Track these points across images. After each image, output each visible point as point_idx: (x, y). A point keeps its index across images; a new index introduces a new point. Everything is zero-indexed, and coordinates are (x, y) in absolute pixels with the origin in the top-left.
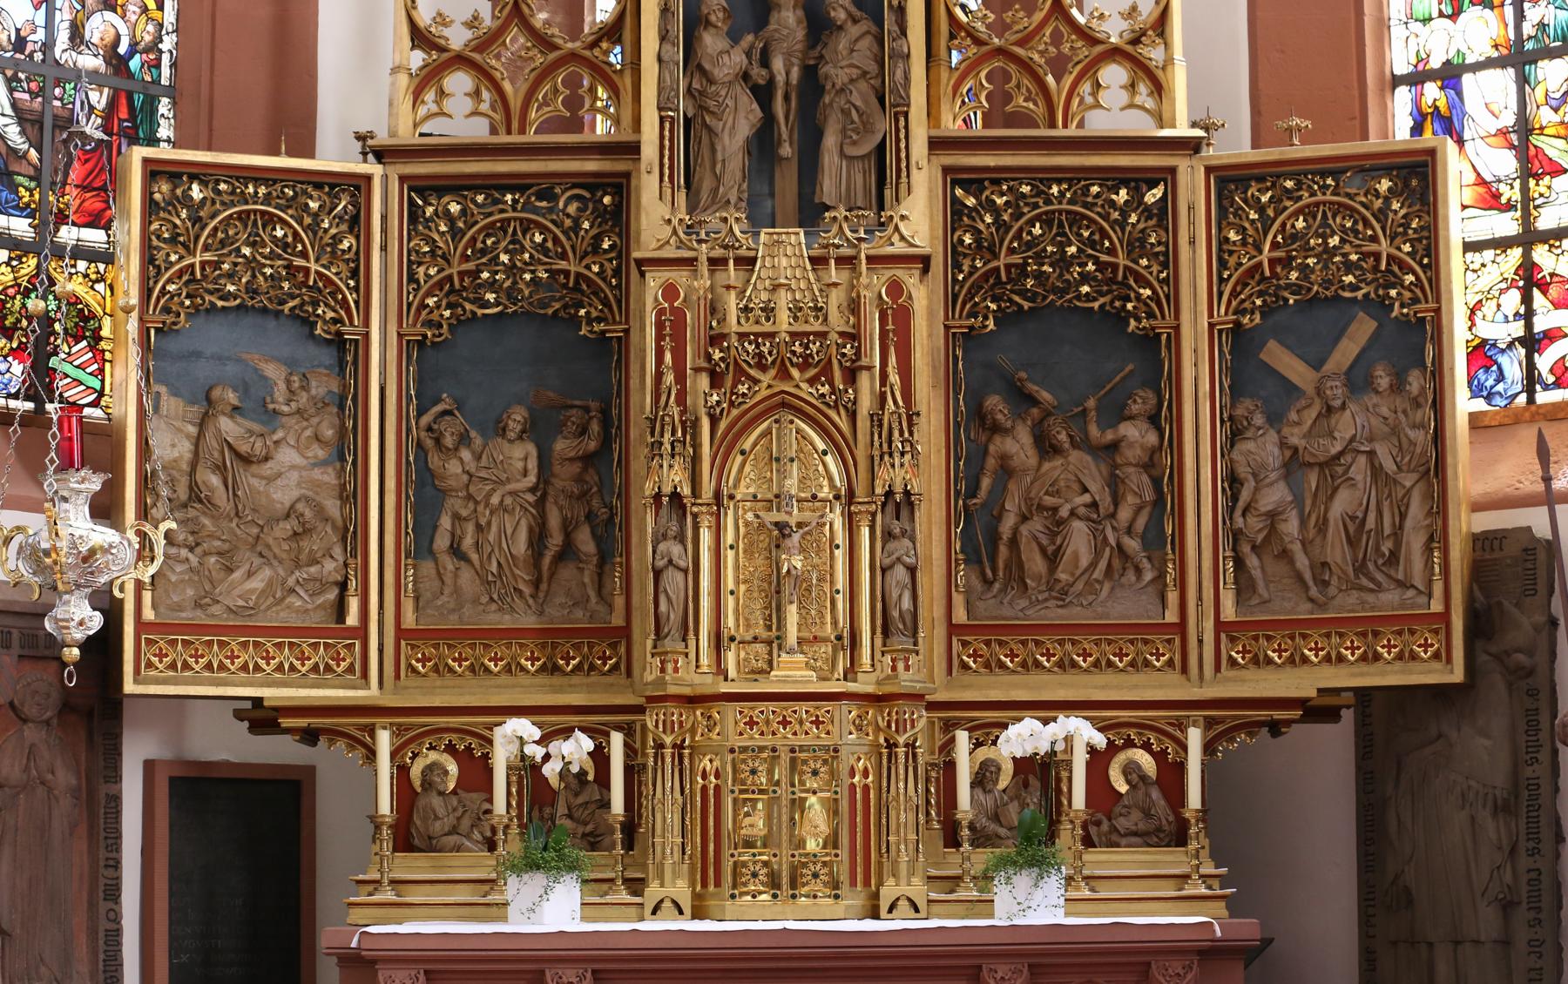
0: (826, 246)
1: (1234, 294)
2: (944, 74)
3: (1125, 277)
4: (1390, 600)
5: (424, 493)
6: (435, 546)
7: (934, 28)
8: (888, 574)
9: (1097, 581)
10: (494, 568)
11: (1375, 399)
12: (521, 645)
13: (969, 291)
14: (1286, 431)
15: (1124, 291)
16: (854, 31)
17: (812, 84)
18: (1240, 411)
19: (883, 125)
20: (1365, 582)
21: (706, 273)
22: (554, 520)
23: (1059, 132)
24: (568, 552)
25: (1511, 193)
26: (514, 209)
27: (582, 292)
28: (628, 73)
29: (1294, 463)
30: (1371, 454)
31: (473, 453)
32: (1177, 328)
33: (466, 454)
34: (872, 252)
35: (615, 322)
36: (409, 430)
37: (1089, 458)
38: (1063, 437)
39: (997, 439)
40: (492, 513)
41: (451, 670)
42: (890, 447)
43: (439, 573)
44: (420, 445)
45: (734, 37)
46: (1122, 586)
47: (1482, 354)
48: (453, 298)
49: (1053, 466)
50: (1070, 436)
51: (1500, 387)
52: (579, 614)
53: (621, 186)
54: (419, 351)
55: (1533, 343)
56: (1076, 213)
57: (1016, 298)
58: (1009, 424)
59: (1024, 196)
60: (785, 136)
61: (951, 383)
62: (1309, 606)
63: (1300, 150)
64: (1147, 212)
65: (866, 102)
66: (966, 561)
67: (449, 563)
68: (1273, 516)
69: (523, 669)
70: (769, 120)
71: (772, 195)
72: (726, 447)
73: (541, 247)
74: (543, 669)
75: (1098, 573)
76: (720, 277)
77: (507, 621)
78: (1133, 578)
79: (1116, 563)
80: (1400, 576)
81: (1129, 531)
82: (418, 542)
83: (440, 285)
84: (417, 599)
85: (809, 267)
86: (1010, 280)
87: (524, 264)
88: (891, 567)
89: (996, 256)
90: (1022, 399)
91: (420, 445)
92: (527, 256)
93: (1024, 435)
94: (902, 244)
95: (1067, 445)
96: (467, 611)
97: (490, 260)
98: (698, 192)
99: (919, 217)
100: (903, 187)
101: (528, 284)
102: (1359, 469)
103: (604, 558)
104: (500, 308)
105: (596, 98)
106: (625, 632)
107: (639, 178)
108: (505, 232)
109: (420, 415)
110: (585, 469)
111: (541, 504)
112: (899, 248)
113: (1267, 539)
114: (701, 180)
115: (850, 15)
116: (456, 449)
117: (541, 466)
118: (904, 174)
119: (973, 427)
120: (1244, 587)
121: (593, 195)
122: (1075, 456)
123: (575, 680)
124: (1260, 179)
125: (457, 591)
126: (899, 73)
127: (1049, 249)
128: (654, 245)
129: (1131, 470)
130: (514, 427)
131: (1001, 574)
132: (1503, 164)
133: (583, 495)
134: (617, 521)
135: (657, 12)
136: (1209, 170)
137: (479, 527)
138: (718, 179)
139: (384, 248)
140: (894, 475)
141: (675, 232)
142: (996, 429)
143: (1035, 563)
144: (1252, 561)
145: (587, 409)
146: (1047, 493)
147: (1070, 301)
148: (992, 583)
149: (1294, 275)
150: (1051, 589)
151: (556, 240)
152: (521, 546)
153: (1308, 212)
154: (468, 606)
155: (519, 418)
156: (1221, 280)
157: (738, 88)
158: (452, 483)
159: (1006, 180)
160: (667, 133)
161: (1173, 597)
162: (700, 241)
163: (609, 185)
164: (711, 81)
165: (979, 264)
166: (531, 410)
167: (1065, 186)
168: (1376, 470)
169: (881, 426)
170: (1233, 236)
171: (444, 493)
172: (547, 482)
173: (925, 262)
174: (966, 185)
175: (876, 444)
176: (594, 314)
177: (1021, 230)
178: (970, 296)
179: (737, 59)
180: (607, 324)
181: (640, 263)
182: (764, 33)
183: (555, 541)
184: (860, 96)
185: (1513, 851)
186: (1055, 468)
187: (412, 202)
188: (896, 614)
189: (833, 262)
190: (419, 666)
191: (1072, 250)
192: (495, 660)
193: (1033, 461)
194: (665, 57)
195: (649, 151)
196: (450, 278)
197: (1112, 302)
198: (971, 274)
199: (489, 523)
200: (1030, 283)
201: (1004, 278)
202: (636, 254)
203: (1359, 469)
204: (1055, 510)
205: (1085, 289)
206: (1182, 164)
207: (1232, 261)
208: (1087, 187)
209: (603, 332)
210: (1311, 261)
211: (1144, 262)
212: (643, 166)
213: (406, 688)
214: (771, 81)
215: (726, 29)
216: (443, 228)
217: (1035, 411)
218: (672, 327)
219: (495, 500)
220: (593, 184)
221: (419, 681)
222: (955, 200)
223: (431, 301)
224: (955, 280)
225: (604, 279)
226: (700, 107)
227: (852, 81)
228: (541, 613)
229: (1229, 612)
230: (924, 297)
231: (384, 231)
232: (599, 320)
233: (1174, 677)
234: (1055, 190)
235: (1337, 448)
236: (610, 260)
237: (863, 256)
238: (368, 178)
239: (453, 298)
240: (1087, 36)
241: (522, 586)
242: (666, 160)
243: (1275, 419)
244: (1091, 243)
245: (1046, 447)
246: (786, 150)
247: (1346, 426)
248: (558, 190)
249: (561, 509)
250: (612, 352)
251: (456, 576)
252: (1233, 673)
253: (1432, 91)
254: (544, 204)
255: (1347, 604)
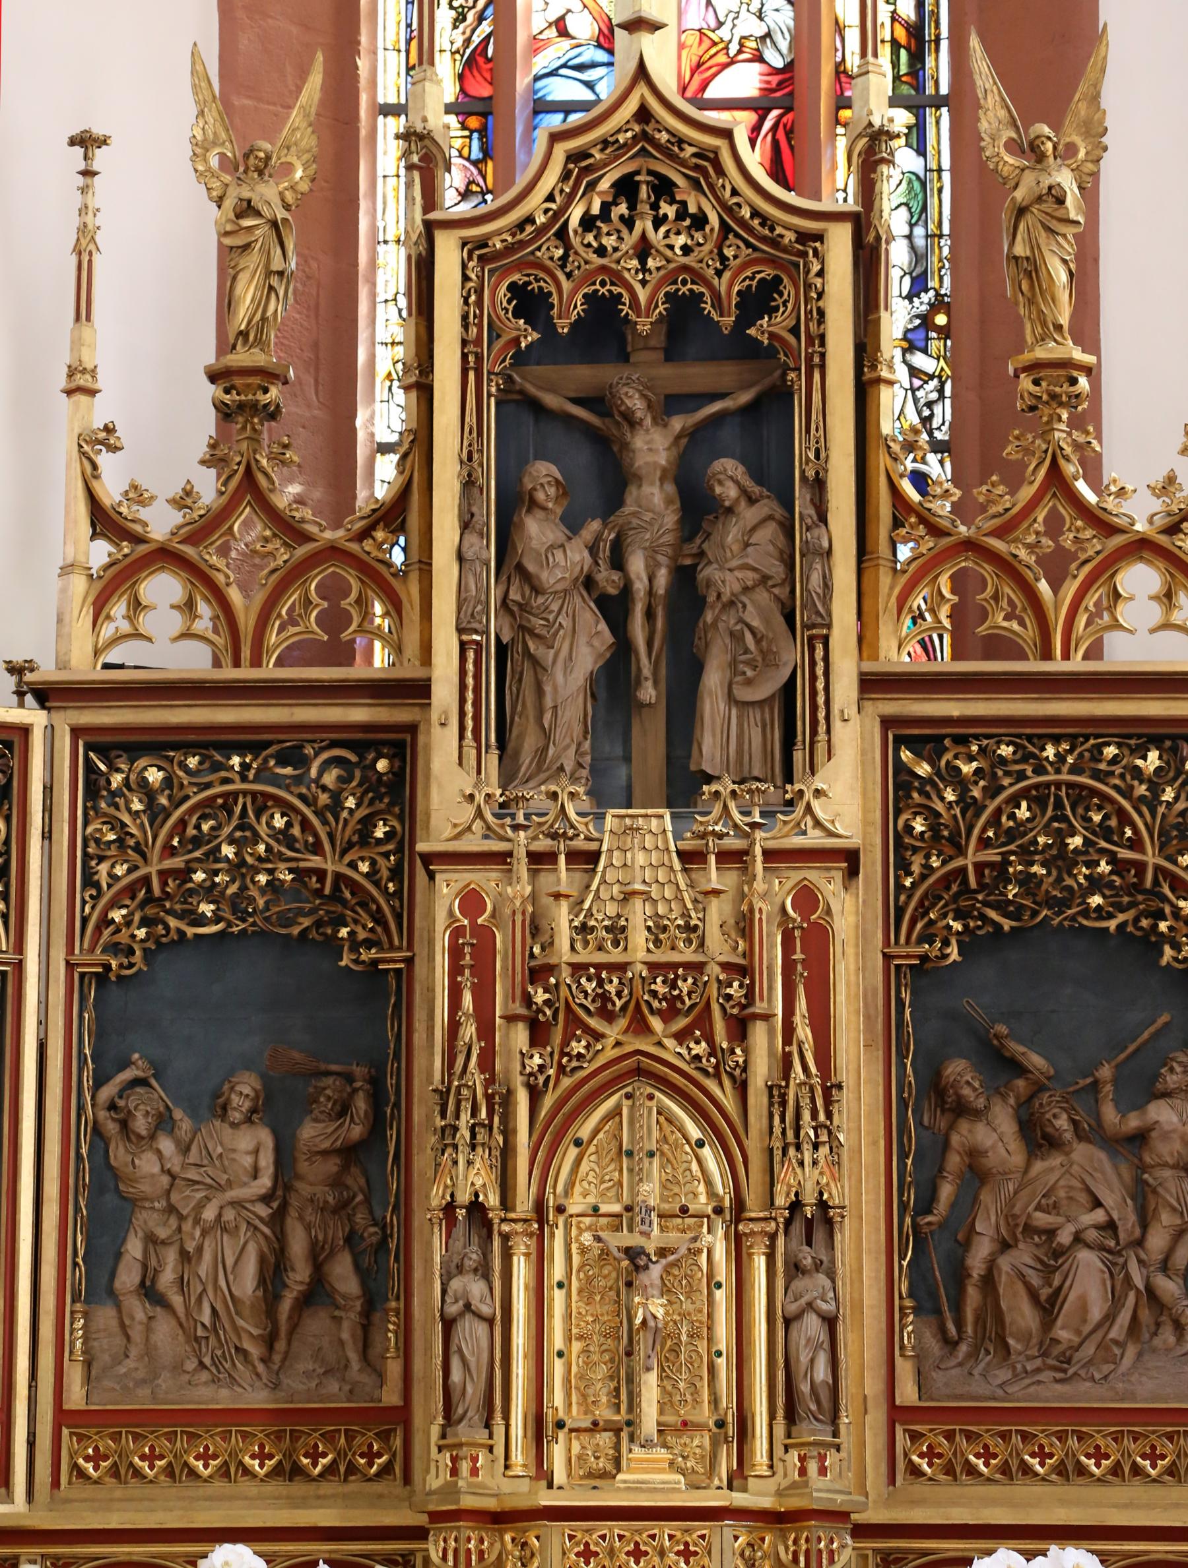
0: (703, 836)
2: (885, 579)
3: (1156, 883)
5: (101, 1203)
6: (117, 1284)
7: (870, 511)
8: (794, 1327)
9: (1116, 1342)
10: (206, 1317)
12: (245, 1435)
13: (921, 903)
15: (1155, 904)
16: (749, 515)
17: (687, 594)
19: (792, 655)
21: (525, 875)
22: (298, 1245)
23: (1057, 665)
24: (317, 1292)
26: (244, 779)
27: (344, 903)
28: (414, 577)
31: (178, 1143)
33: (166, 1145)
34: (772, 844)
35: (392, 948)
36: (81, 1108)
37: (1102, 1155)
38: (1062, 1122)
39: (964, 1125)
40: (204, 1233)
41: (137, 1473)
42: (797, 1136)
43: (123, 1326)
44: (97, 1131)
45: (572, 524)
46: (1154, 1350)
48: (150, 911)
49: (1048, 1167)
50: (1074, 1122)
52: (333, 1386)
53: (403, 745)
54: (99, 990)
56: (1082, 787)
57: (992, 914)
58: (981, 1103)
59: (1003, 761)
60: (646, 671)
61: (894, 1040)
65: (767, 621)
66: (917, 1311)
67: (138, 1309)
69: (247, 1471)
70: (623, 648)
71: (627, 759)
72: (553, 1134)
73: (283, 834)
74: (277, 1472)
75: (1117, 1331)
76: (546, 881)
77: (224, 1398)
78: (1172, 1339)
79: (1145, 1315)
81: (1165, 1266)
82: (92, 1277)
83: (131, 890)
84: (88, 1364)
85: (677, 865)
86: (982, 887)
87: (259, 860)
88: (799, 1316)
89: (961, 851)
90: (1002, 1066)
91: (97, 1131)
92: (261, 848)
93: (1004, 1120)
94: (818, 832)
95: (1068, 1136)
96: (165, 1382)
97: (207, 855)
98: (517, 754)
99: (844, 792)
100: (821, 747)
101: (263, 891)
103: (372, 1302)
104: (221, 926)
105: (367, 615)
106: (402, 1415)
107: (429, 732)
108: (230, 813)
109: (98, 1084)
110: (345, 1168)
111: (278, 1219)
112: (814, 839)
114: (521, 736)
115: (744, 491)
116: (152, 1137)
117: (278, 1163)
118: (822, 728)
119: (925, 1109)
121: (362, 757)
122: (1082, 1152)
123: (326, 1488)
125: (149, 1351)
126: (816, 579)
127: (1041, 840)
128: (449, 832)
129: (1167, 1173)
130: (240, 1103)
131: (970, 1330)
133: (343, 1207)
134: (393, 1245)
135: (457, 487)
137: (185, 1256)
138: (547, 735)
139: (47, 835)
140: (803, 1178)
141: (479, 814)
142: (962, 1110)
143: (1022, 1314)
145: (349, 1078)
146: (1038, 1208)
147: (1073, 918)
148: (956, 1344)
150: (1045, 1355)
151: (306, 825)
152: (247, 1283)
154: (165, 1374)
155: (246, 1090)
157: (578, 600)
158: (145, 1188)
159: (976, 737)
160: (470, 667)
162: (516, 828)
163: (384, 743)
164: (537, 590)
165: (935, 862)
166: (264, 1077)
167: (1065, 746)
169: (783, 1103)
171: (133, 1203)
172: (288, 1188)
173: (850, 860)
174: (915, 744)
175: (777, 1130)
176: (362, 935)
177: (998, 812)
178: (923, 909)
179: (576, 557)
180: (381, 950)
181: (428, 859)
182: (617, 519)
183: (299, 1275)
184: (758, 612)
186: (1052, 1169)
187: (90, 767)
188: (805, 1388)
189: (712, 859)
190: (89, 1467)
191: (1076, 842)
192: (205, 1457)
193: (1018, 1158)
194: (469, 554)
195: (444, 692)
196: (146, 880)
197: (1136, 920)
198: (923, 877)
199: (200, 1249)
200: (1012, 891)
201: (973, 884)
202: (421, 847)
204: (1051, 1233)
205: (1096, 900)
208: (1099, 748)
209: (375, 962)
212: (435, 715)
213: (68, 1501)
214: (627, 590)
215: (559, 511)
216: (137, 806)
217: (1020, 1083)
218: (474, 954)
219: (209, 1214)
220: (363, 741)
221: (89, 1490)
222: (901, 768)
223: (117, 915)
224: (899, 887)
225: (377, 884)
226: (522, 627)
227: (746, 589)
228: (276, 1386)
230: (852, 916)
231: (48, 809)
232: (369, 944)
234: (1050, 752)
236: (386, 855)
237: (758, 851)
238: (25, 731)
239: (150, 911)
240: (1103, 524)
241: (247, 1345)
242: (469, 707)
244: (1105, 831)
245: (1037, 1138)
246: (648, 692)
248: (308, 751)
249: (308, 1228)
250: (387, 992)
251: (148, 1329)
254: (288, 771)
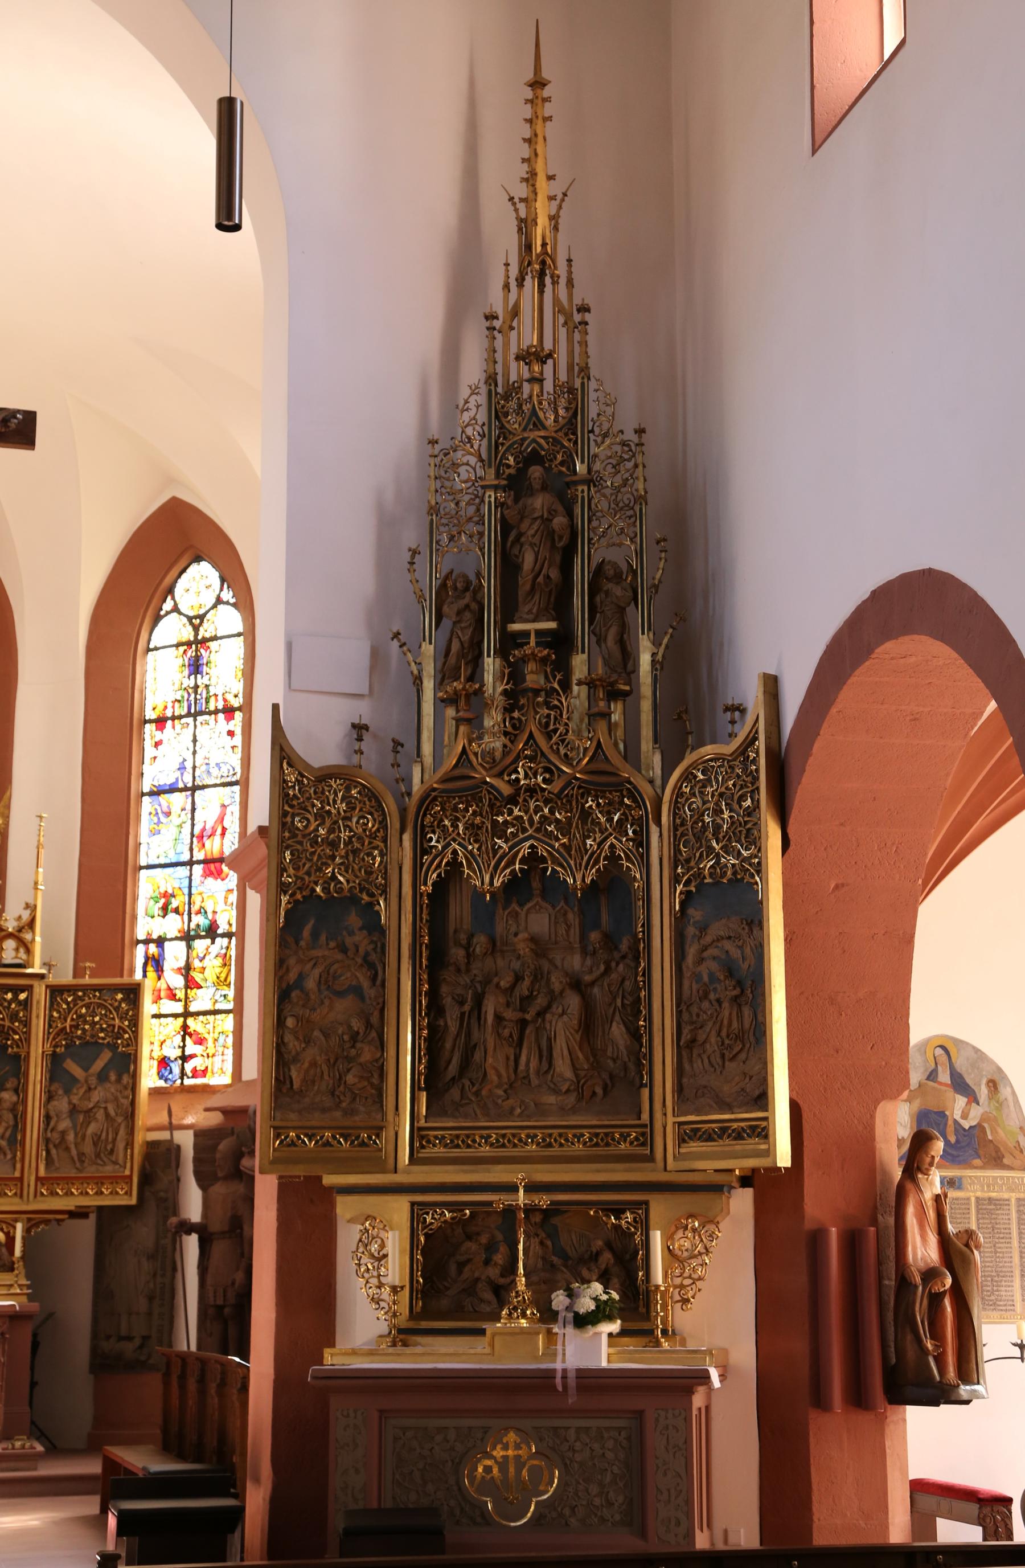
1: (54, 1039)
4: (109, 1169)
11: (109, 1085)
14: (72, 1097)
18: (53, 1088)
20: (99, 1162)
25: (180, 994)
29: (74, 1110)
30: (106, 1108)
32: (28, 1053)
47: (164, 1063)
51: (170, 1076)
55: (185, 1058)
62: (75, 1171)
63: (87, 980)
64: (20, 1003)
68: (63, 1133)
80: (114, 1159)
102: (100, 1115)
113: (60, 1143)
120: (49, 1161)
124: (69, 991)
132: (177, 982)
136: (47, 987)
144: (54, 1151)
149: (79, 1032)
153: (87, 1006)
156: (49, 1033)
161: (18, 1166)
168: (107, 1115)
170: (55, 1014)
185: (155, 1275)
203: (100, 1115)
206: (36, 984)
207: (54, 1025)
210: (87, 1027)
211: (17, 1024)
229: (42, 1172)
233: (17, 1200)
235: (91, 1105)
243: (68, 1092)
247: (96, 1096)
252: (42, 1199)
253: (153, 949)
255: (91, 1171)
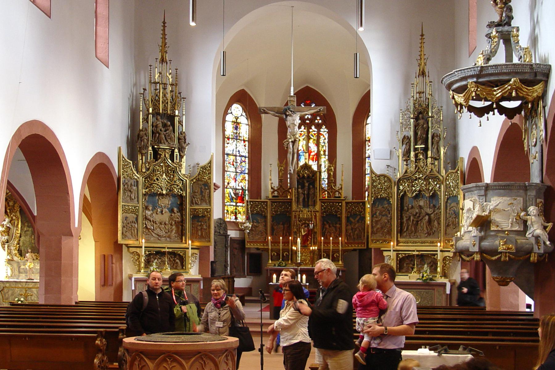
53: (291, 202)
99: (318, 207)
195: (293, 200)
245: (330, 227)
